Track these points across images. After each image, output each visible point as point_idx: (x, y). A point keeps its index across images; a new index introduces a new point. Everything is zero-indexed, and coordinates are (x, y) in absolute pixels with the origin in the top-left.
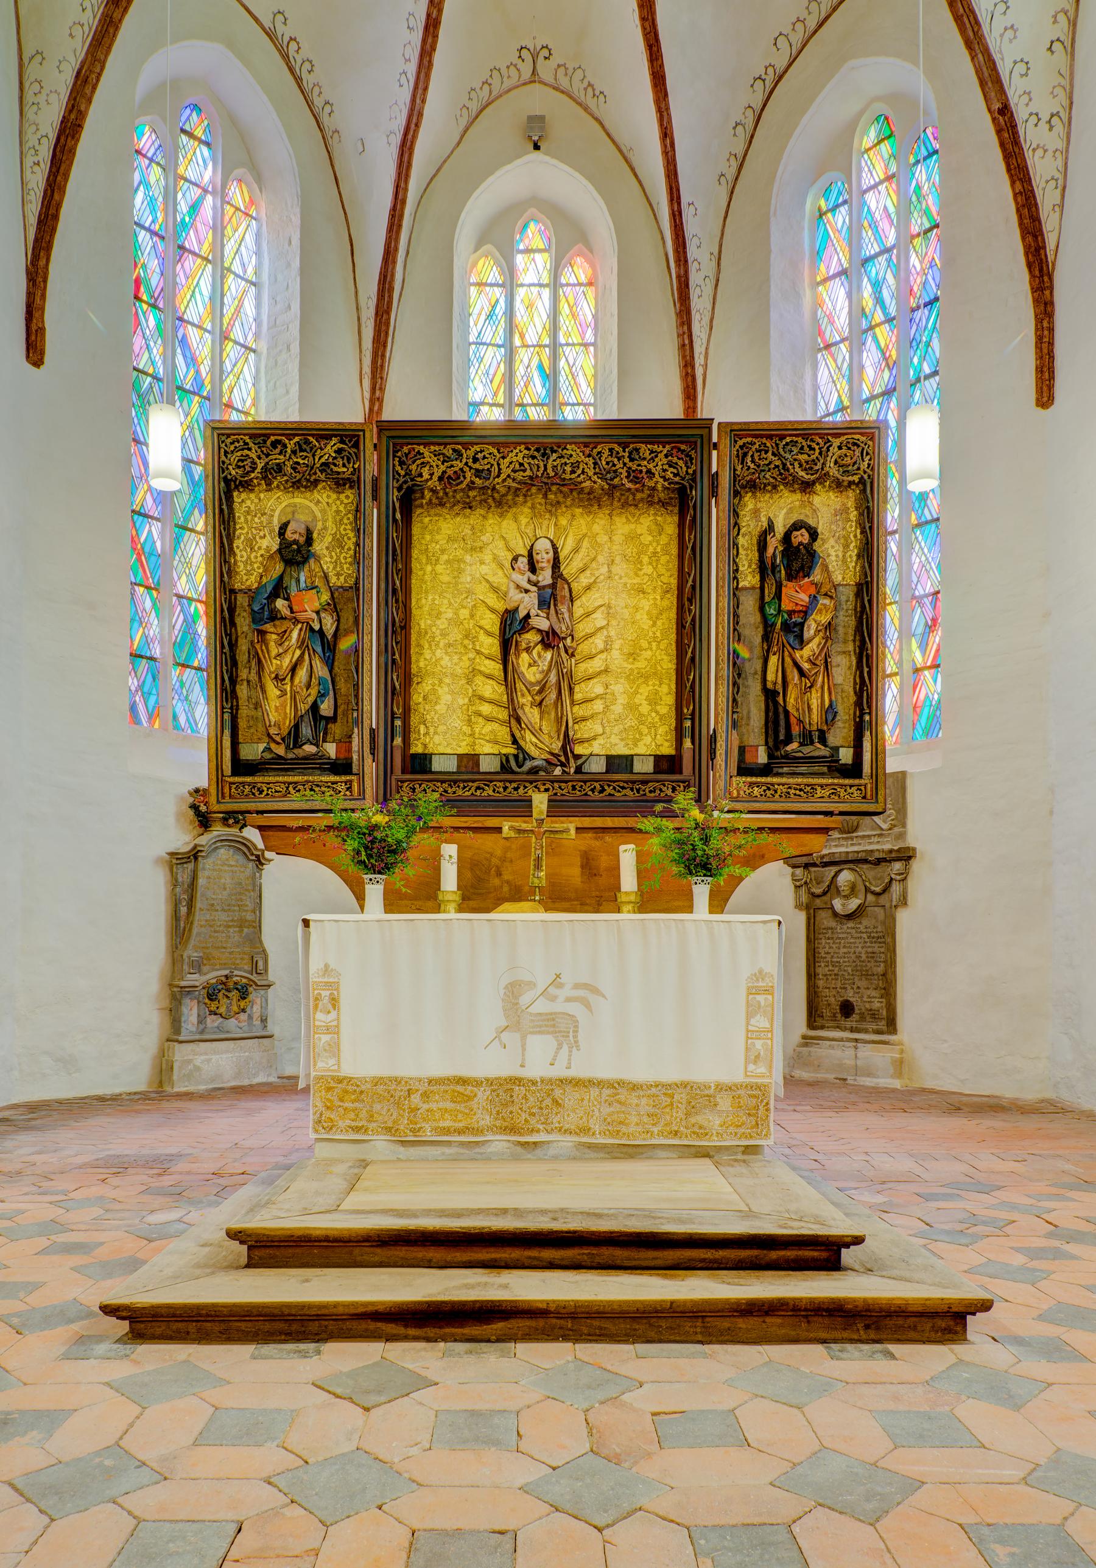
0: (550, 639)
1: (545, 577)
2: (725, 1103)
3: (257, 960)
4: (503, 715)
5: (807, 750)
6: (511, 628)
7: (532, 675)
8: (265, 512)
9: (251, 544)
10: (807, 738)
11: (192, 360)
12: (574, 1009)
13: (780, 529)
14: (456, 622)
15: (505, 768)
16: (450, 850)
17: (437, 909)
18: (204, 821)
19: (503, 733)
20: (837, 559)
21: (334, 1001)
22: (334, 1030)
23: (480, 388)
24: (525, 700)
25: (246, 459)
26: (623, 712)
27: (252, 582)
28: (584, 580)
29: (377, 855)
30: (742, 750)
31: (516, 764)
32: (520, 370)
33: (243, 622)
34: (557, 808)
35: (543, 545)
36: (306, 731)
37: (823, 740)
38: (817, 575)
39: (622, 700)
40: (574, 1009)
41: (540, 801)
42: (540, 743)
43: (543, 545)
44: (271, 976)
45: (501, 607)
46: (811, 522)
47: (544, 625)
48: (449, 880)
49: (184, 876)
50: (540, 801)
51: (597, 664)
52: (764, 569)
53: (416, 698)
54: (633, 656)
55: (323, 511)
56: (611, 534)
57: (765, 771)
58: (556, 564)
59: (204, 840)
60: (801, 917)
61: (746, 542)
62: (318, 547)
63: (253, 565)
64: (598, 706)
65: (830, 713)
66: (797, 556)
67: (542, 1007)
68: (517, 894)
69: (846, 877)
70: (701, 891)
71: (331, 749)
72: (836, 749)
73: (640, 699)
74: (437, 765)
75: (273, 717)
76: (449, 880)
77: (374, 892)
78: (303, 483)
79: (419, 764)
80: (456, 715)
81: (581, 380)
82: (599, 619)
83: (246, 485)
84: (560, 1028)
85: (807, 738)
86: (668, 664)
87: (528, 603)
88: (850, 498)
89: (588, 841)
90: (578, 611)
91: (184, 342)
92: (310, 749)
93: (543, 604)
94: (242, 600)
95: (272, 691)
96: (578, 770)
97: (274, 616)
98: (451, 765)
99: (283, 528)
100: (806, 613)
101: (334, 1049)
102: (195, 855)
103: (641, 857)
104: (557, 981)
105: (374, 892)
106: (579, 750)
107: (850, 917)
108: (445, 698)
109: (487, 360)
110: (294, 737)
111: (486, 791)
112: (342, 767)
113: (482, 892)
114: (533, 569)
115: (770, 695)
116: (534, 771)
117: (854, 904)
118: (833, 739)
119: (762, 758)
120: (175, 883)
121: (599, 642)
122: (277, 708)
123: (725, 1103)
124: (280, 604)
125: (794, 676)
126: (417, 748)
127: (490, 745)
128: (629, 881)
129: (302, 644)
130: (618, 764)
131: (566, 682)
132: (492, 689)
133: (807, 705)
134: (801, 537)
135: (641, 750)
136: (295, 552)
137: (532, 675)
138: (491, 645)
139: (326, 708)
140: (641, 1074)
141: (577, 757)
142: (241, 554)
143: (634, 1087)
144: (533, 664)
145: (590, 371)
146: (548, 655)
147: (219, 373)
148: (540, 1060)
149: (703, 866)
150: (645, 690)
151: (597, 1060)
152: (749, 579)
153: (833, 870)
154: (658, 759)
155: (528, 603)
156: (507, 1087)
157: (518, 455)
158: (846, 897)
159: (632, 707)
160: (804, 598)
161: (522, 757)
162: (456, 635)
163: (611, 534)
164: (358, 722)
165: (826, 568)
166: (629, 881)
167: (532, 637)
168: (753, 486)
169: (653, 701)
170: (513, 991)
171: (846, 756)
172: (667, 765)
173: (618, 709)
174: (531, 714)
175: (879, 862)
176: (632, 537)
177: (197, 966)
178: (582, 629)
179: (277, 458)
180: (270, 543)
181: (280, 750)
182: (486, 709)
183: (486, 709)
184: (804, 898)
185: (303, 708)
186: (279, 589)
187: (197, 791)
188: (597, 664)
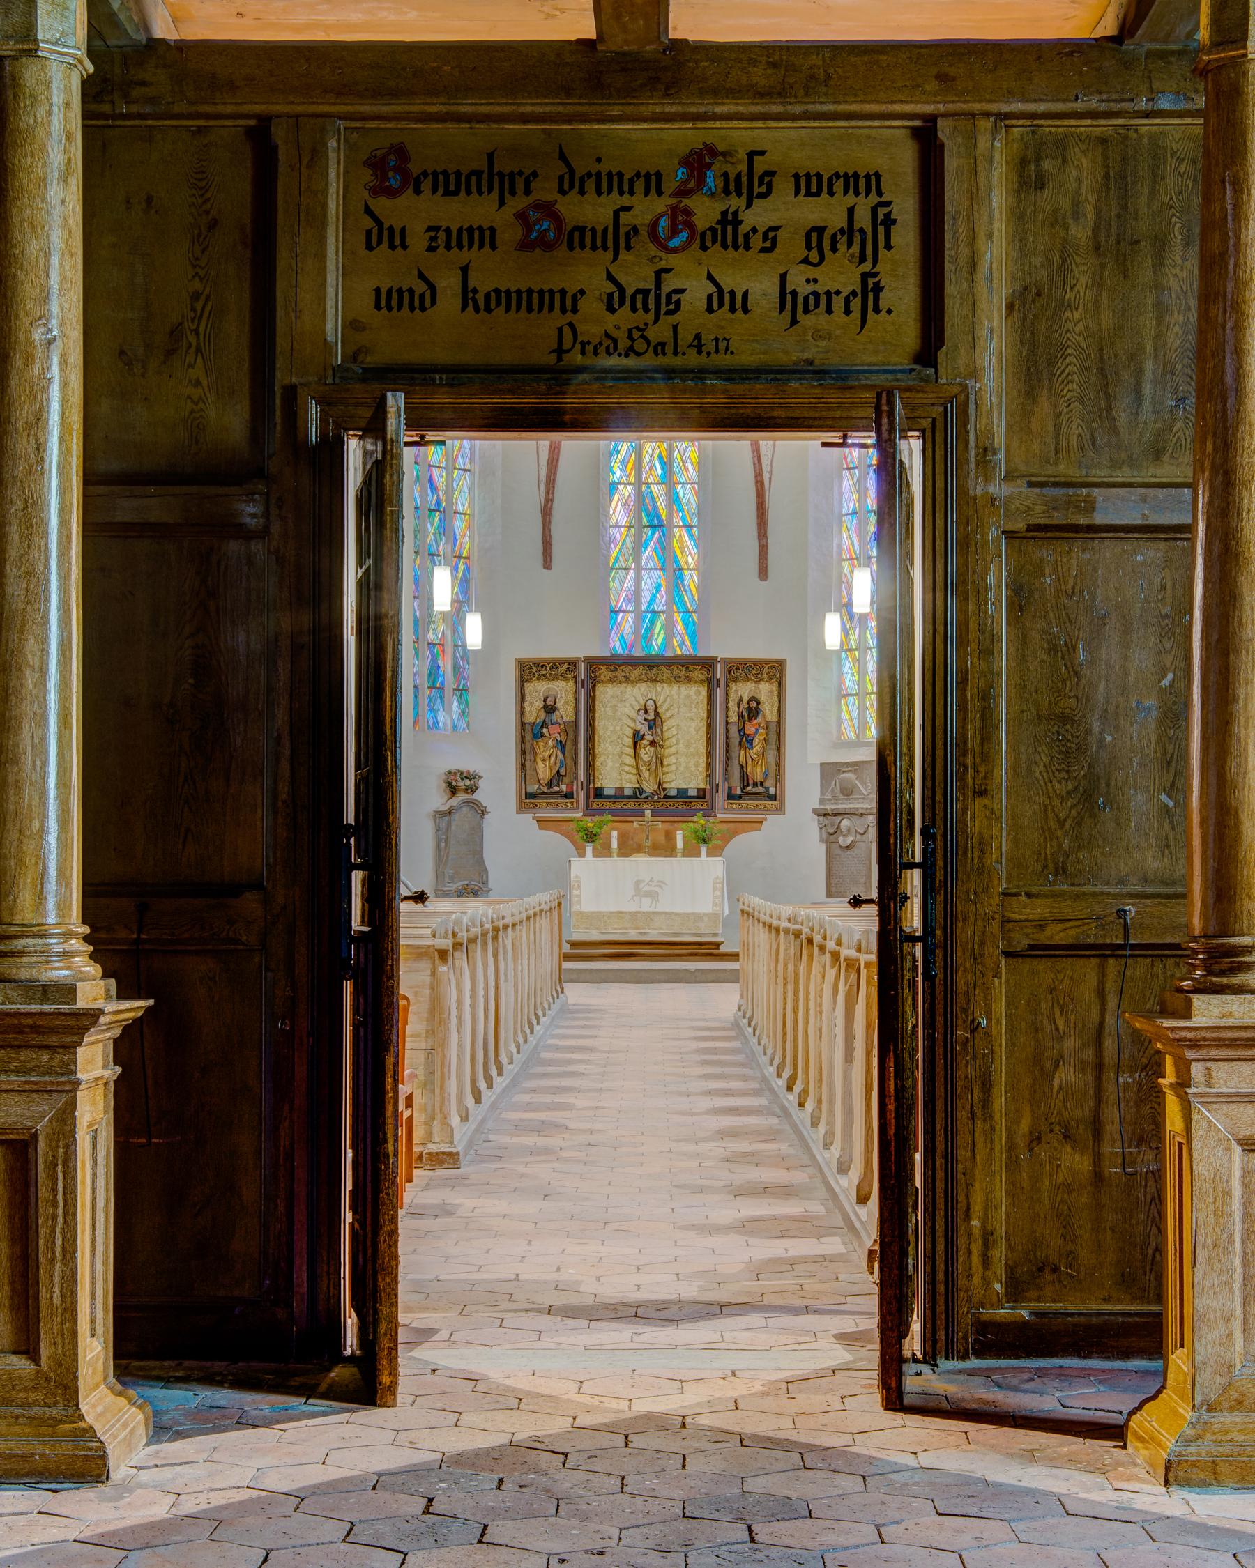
0: (653, 743)
1: (651, 716)
2: (706, 919)
3: (483, 873)
4: (634, 771)
5: (754, 790)
6: (637, 738)
7: (646, 758)
8: (538, 689)
9: (531, 704)
10: (755, 784)
11: (434, 489)
12: (657, 889)
13: (745, 699)
14: (614, 732)
15: (635, 793)
16: (615, 834)
17: (610, 856)
18: (453, 791)
19: (634, 778)
20: (769, 711)
21: (579, 887)
22: (579, 896)
23: (618, 473)
24: (643, 768)
25: (530, 670)
26: (685, 768)
27: (532, 719)
28: (668, 714)
29: (591, 837)
30: (730, 788)
31: (638, 794)
32: (647, 459)
33: (528, 736)
34: (655, 813)
35: (650, 703)
36: (555, 781)
37: (762, 784)
38: (759, 719)
39: (684, 765)
40: (657, 889)
41: (648, 813)
42: (649, 787)
43: (650, 703)
44: (491, 885)
45: (632, 725)
46: (758, 696)
47: (651, 738)
48: (614, 844)
49: (443, 825)
50: (648, 813)
51: (673, 750)
52: (741, 716)
53: (597, 764)
54: (688, 746)
55: (562, 690)
56: (679, 694)
57: (740, 797)
58: (656, 708)
59: (455, 802)
60: (823, 847)
61: (732, 704)
62: (558, 705)
63: (533, 713)
64: (674, 767)
65: (766, 776)
66: (753, 711)
67: (647, 888)
68: (639, 849)
69: (845, 823)
70: (704, 849)
71: (564, 788)
72: (767, 789)
73: (691, 764)
74: (606, 793)
75: (541, 775)
76: (614, 844)
77: (589, 850)
78: (554, 678)
79: (599, 793)
80: (615, 772)
81: (689, 466)
82: (674, 731)
83: (530, 680)
84: (653, 895)
85: (755, 784)
86: (703, 750)
87: (644, 729)
88: (775, 687)
89: (667, 826)
90: (665, 728)
91: (431, 480)
92: (556, 789)
93: (650, 728)
94: (528, 727)
95: (541, 765)
96: (666, 797)
97: (542, 735)
98: (612, 793)
99: (545, 700)
100: (755, 735)
101: (579, 902)
102: (450, 812)
103: (684, 837)
104: (651, 880)
105: (589, 850)
106: (665, 786)
107: (848, 847)
108: (610, 764)
109: (623, 452)
110: (550, 784)
111: (629, 803)
112: (568, 795)
113: (628, 848)
114: (646, 712)
115: (742, 767)
116: (646, 798)
117: (850, 839)
118: (766, 784)
119: (739, 792)
120: (438, 829)
121: (674, 740)
122: (544, 772)
123: (706, 919)
124: (545, 731)
125: (750, 761)
126: (598, 785)
127: (629, 785)
128: (680, 844)
129: (553, 747)
130: (682, 793)
131: (660, 761)
132: (630, 760)
133: (756, 773)
134: (753, 704)
135: (691, 786)
136: (550, 709)
137: (646, 758)
138: (630, 742)
139: (562, 772)
140: (678, 910)
141: (664, 789)
142: (527, 708)
143: (677, 914)
144: (646, 754)
145: (695, 459)
146: (653, 749)
147: (450, 491)
148: (646, 905)
149: (704, 841)
150: (693, 761)
151: (664, 906)
152: (733, 718)
153: (839, 818)
154: (698, 790)
155: (644, 729)
156: (634, 915)
157: (640, 670)
158: (845, 836)
159: (687, 768)
160: (753, 730)
161: (641, 791)
162: (614, 737)
163: (679, 694)
164: (576, 778)
165: (764, 716)
166: (680, 844)
167: (644, 742)
168: (736, 680)
169: (697, 765)
170: (637, 883)
171: (772, 791)
172: (701, 794)
173: (682, 769)
174: (646, 774)
175: (862, 814)
176: (688, 696)
177: (452, 879)
178: (666, 735)
179: (543, 672)
180: (539, 704)
181: (545, 790)
182: (627, 768)
183: (627, 768)
184: (825, 836)
185: (554, 772)
186: (544, 724)
187: (450, 772)
188: (673, 750)
